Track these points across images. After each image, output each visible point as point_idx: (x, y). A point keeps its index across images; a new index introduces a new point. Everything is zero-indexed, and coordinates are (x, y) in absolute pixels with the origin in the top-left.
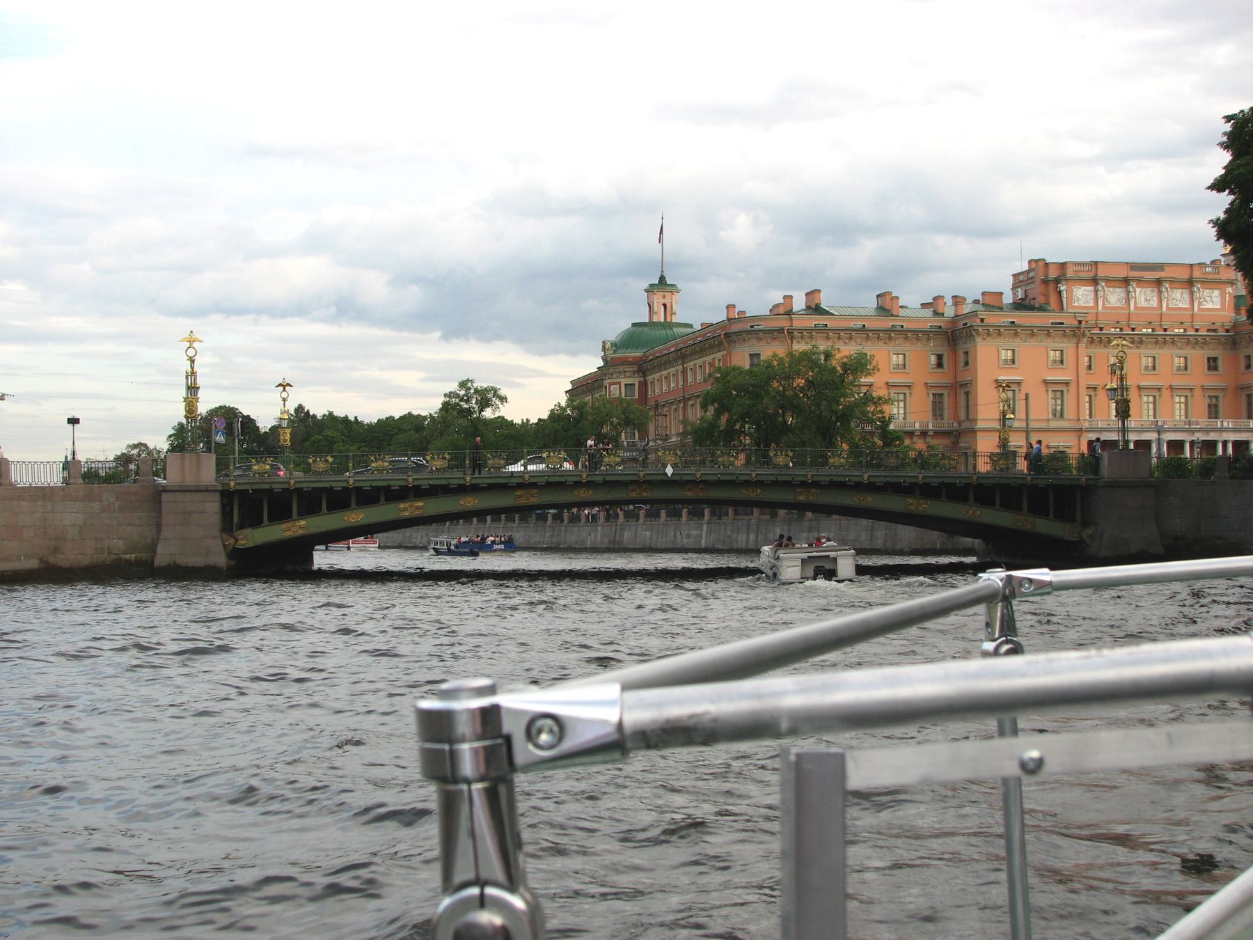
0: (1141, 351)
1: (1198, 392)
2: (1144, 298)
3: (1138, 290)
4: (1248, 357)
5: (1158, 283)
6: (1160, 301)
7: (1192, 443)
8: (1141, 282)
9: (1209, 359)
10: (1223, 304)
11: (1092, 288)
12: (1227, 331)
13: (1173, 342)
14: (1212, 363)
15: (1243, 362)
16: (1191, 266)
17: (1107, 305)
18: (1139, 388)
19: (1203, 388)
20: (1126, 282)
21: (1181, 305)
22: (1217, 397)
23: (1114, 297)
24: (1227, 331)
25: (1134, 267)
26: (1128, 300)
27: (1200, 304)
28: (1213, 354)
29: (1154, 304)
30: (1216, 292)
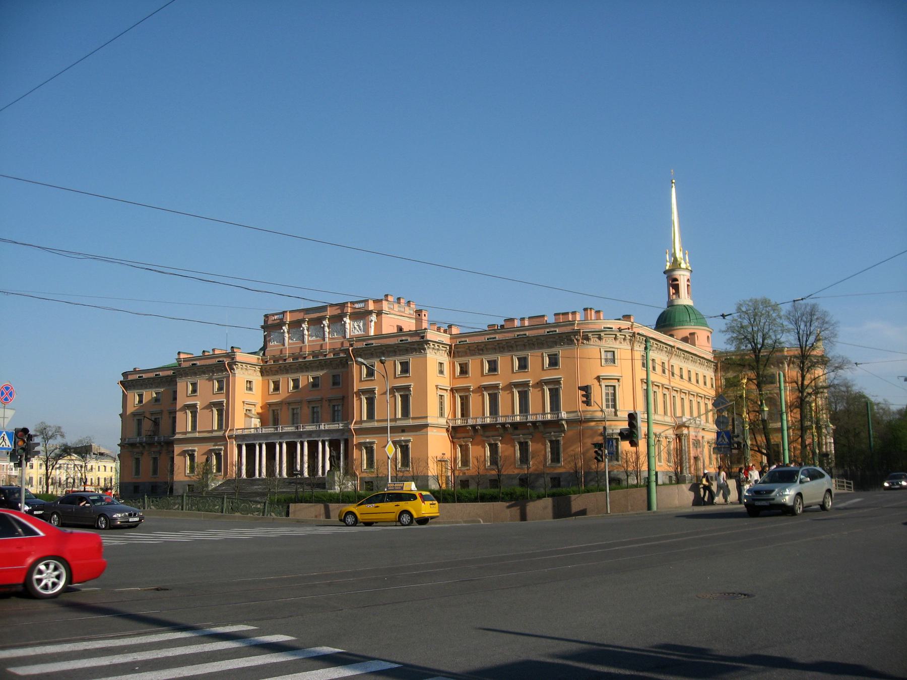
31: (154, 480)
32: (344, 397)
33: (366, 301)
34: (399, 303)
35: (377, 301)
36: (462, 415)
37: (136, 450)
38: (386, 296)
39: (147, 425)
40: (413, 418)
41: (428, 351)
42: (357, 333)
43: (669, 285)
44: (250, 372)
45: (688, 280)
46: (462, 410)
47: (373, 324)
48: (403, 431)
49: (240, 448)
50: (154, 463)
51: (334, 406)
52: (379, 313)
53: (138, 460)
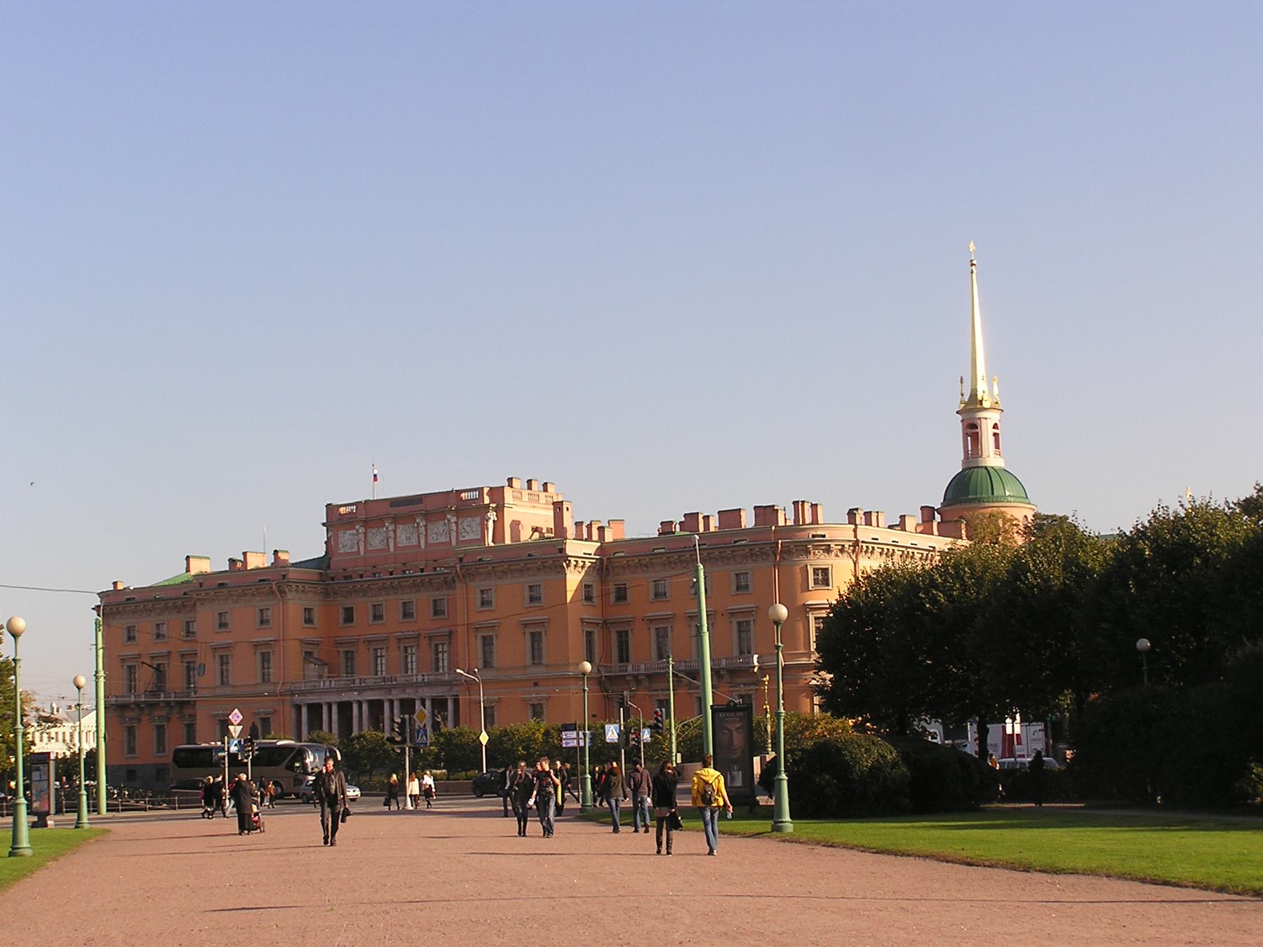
2: (405, 536)
5: (410, 518)
8: (396, 520)
23: (376, 540)
30: (478, 520)
31: (131, 762)
32: (451, 632)
33: (481, 490)
34: (530, 488)
35: (497, 493)
36: (621, 660)
37: (129, 714)
38: (510, 480)
39: (145, 676)
41: (568, 571)
43: (966, 435)
44: (309, 595)
45: (995, 426)
46: (621, 652)
47: (491, 524)
48: (536, 684)
49: (298, 708)
50: (188, 732)
51: (437, 646)
52: (500, 510)
53: (131, 731)
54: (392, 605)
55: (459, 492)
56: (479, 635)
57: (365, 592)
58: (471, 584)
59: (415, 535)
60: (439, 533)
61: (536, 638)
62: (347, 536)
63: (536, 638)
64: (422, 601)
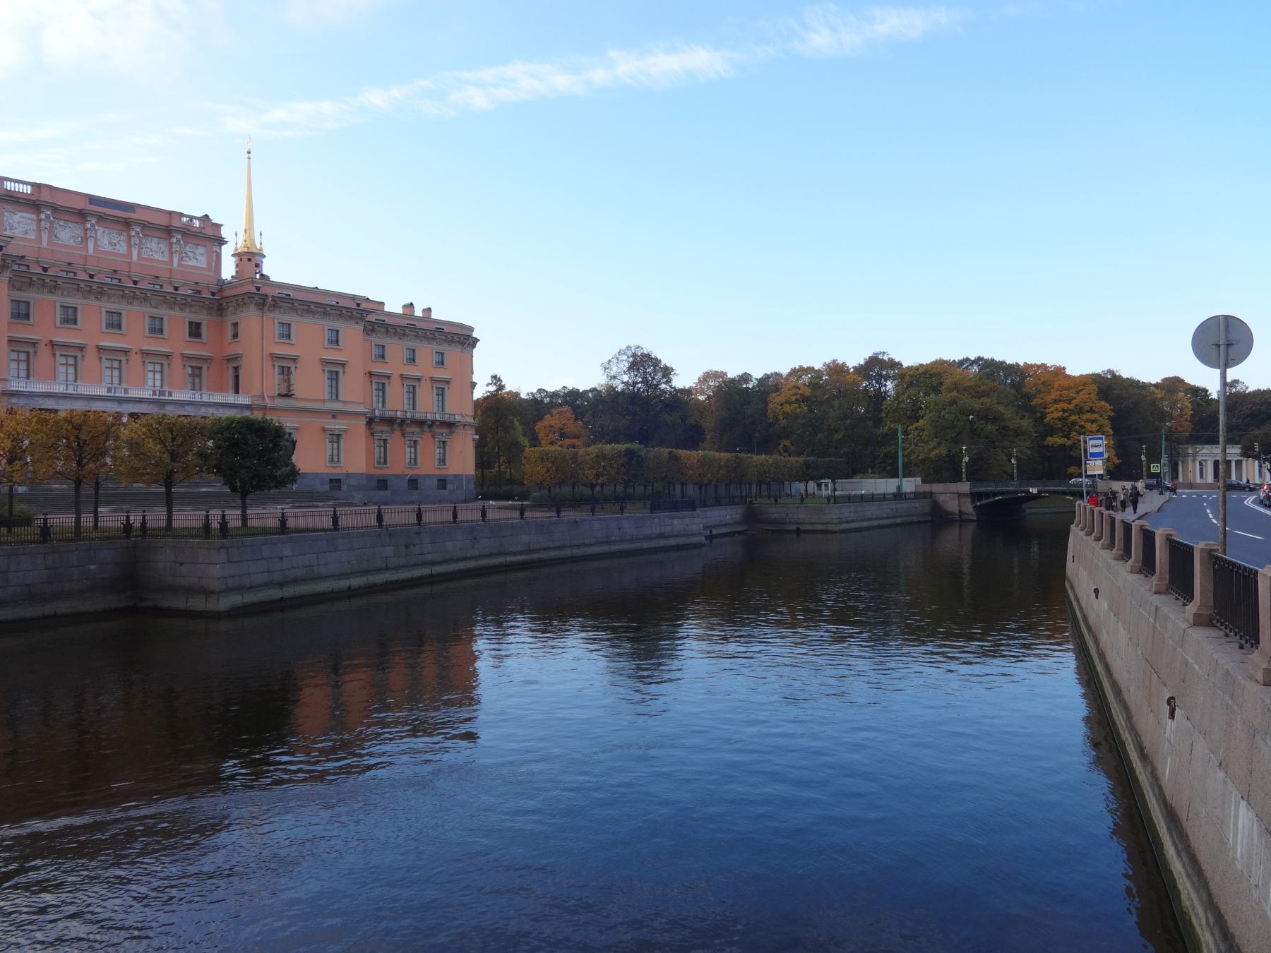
0: (102, 304)
1: (177, 362)
2: (108, 242)
3: (100, 230)
4: (235, 325)
5: (127, 224)
6: (130, 246)
7: (132, 415)
8: (101, 218)
9: (191, 323)
10: (209, 263)
11: (34, 217)
12: (213, 294)
13: (146, 299)
14: (195, 330)
15: (229, 331)
16: (170, 213)
17: (55, 241)
18: (99, 348)
19: (183, 356)
20: (82, 215)
21: (156, 257)
22: (200, 368)
23: (67, 234)
24: (213, 294)
25: (94, 200)
26: (85, 239)
27: (181, 259)
28: (196, 318)
29: (122, 248)
30: (201, 250)
40: (345, 402)
42: (190, 263)
48: (334, 417)
54: (93, 313)
55: (181, 215)
56: (277, 364)
57: (54, 288)
58: (272, 315)
59: (124, 245)
60: (155, 251)
61: (334, 377)
62: (17, 217)
63: (334, 377)
64: (136, 317)
